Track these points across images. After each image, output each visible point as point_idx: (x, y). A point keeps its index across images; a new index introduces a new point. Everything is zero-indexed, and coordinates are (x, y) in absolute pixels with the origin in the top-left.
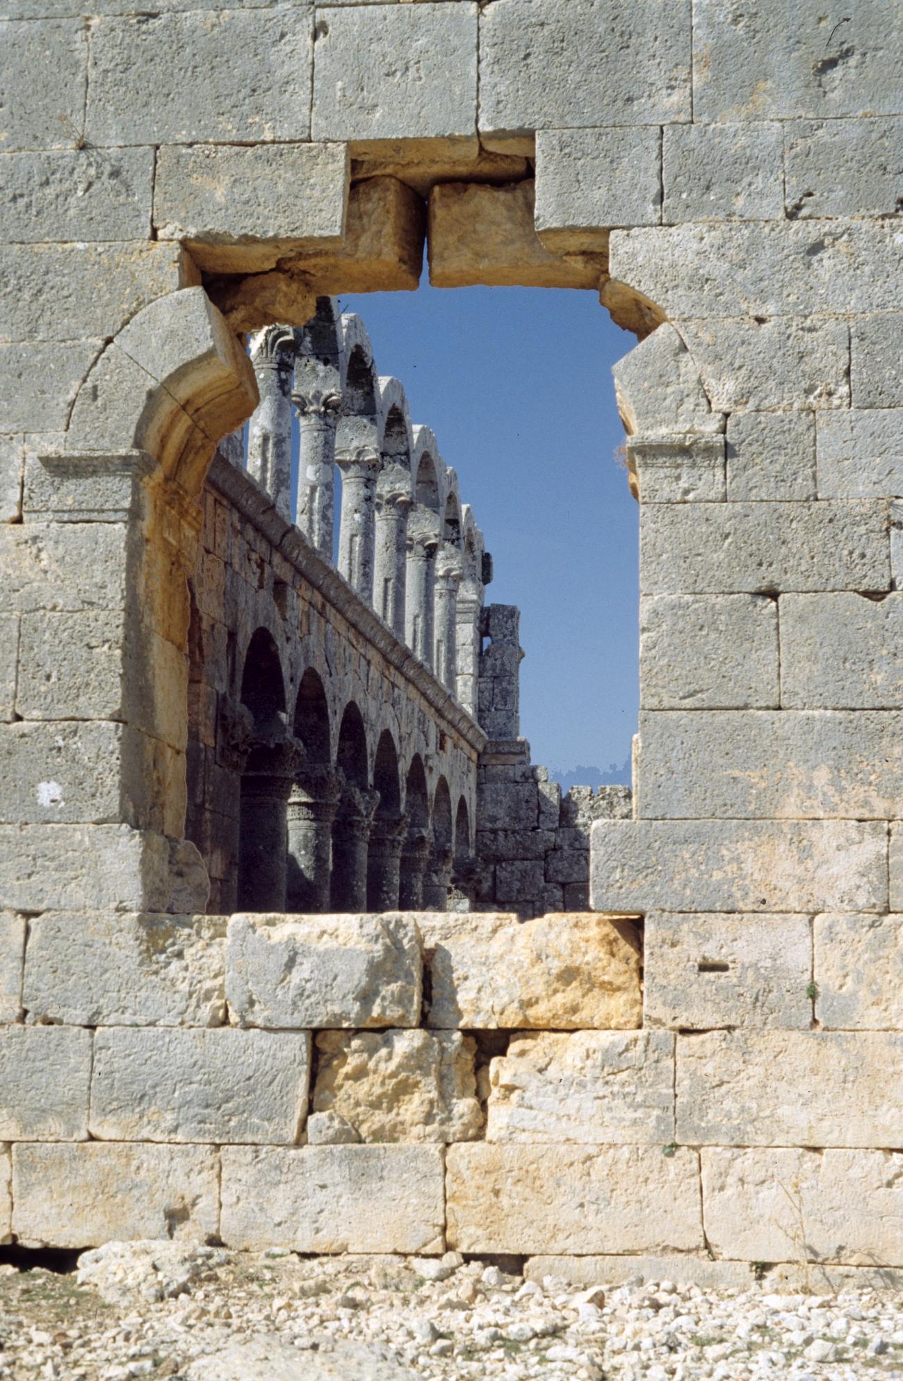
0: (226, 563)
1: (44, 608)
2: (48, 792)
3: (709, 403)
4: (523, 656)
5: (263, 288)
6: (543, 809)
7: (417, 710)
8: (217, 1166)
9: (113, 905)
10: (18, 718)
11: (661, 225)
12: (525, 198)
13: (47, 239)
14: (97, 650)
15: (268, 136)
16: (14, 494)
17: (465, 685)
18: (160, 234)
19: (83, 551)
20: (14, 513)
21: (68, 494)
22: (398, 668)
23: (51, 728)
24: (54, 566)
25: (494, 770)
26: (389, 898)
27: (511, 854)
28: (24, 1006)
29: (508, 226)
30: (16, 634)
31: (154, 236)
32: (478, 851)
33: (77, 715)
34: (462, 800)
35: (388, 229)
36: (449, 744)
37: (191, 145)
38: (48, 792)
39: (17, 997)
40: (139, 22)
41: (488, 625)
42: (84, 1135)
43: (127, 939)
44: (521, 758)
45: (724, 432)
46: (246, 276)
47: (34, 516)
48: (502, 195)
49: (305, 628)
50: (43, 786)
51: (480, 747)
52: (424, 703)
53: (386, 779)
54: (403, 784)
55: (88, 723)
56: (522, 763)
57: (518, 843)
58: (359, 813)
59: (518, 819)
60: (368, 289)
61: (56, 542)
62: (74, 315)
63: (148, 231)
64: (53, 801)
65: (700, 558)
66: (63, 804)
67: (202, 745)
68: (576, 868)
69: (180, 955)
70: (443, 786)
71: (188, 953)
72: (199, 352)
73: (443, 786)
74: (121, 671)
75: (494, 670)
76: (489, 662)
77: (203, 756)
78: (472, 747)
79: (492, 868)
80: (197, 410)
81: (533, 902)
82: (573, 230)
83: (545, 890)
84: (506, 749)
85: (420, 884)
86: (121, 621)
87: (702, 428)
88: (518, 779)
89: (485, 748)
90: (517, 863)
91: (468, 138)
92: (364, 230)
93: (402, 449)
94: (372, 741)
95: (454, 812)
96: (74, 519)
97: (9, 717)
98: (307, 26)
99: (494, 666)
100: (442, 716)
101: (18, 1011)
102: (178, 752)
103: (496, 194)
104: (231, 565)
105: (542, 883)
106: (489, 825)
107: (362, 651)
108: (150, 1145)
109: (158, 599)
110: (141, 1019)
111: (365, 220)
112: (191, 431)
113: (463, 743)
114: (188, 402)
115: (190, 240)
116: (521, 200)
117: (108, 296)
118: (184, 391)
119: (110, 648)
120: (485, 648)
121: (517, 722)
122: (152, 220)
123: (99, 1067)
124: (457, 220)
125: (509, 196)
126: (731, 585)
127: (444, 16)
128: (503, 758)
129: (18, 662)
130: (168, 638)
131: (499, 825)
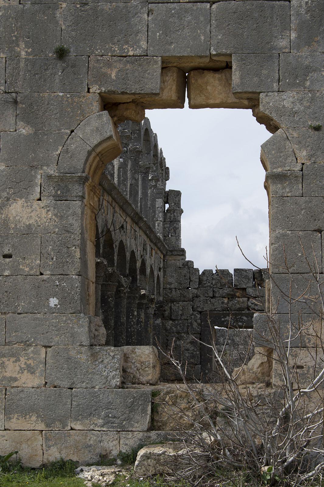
1: (50, 232)
2: (53, 302)
3: (297, 159)
5: (127, 109)
6: (192, 279)
7: (143, 240)
8: (119, 439)
9: (78, 344)
10: (41, 274)
11: (279, 91)
12: (225, 76)
13: (47, 91)
14: (71, 249)
15: (131, 53)
16: (38, 189)
18: (91, 90)
19: (64, 212)
20: (38, 196)
21: (58, 190)
23: (54, 278)
24: (54, 217)
28: (46, 381)
29: (220, 88)
30: (40, 242)
31: (88, 92)
32: (164, 297)
33: (64, 273)
34: (158, 275)
35: (174, 87)
36: (154, 252)
37: (102, 56)
38: (53, 302)
39: (43, 378)
40: (80, 6)
41: (168, 199)
42: (69, 428)
43: (84, 357)
44: (182, 257)
45: (302, 170)
46: (120, 103)
47: (45, 198)
48: (217, 76)
49: (106, 212)
50: (51, 299)
51: (165, 254)
53: (133, 271)
54: (138, 272)
55: (67, 276)
56: (182, 259)
58: (123, 286)
59: (180, 284)
60: (165, 108)
61: (54, 208)
62: (59, 121)
63: (86, 90)
64: (55, 305)
65: (293, 217)
66: (59, 306)
68: (206, 305)
69: (102, 361)
70: (152, 271)
71: (106, 361)
72: (106, 137)
73: (152, 271)
74: (80, 257)
76: (169, 215)
78: (162, 253)
79: (170, 304)
80: (102, 155)
81: (187, 320)
82: (246, 92)
83: (193, 314)
84: (176, 253)
85: (143, 314)
86: (80, 238)
87: (294, 169)
88: (181, 266)
89: (167, 253)
91: (206, 56)
92: (165, 88)
93: (137, 128)
95: (156, 282)
96: (61, 199)
97: (38, 273)
98: (145, 9)
99: (170, 217)
100: (151, 241)
101: (44, 383)
102: (93, 283)
103: (215, 75)
105: (191, 312)
108: (94, 431)
109: (88, 226)
110: (89, 386)
111: (166, 84)
112: (98, 162)
113: (159, 252)
114: (100, 152)
115: (102, 93)
116: (224, 77)
117: (72, 114)
118: (99, 150)
119: (75, 248)
120: (166, 209)
121: (180, 241)
122: (88, 85)
123: (74, 403)
124: (200, 85)
125: (220, 76)
126: (304, 228)
127: (197, 8)
128: (174, 257)
129: (41, 253)
130: (91, 241)
131: (173, 286)
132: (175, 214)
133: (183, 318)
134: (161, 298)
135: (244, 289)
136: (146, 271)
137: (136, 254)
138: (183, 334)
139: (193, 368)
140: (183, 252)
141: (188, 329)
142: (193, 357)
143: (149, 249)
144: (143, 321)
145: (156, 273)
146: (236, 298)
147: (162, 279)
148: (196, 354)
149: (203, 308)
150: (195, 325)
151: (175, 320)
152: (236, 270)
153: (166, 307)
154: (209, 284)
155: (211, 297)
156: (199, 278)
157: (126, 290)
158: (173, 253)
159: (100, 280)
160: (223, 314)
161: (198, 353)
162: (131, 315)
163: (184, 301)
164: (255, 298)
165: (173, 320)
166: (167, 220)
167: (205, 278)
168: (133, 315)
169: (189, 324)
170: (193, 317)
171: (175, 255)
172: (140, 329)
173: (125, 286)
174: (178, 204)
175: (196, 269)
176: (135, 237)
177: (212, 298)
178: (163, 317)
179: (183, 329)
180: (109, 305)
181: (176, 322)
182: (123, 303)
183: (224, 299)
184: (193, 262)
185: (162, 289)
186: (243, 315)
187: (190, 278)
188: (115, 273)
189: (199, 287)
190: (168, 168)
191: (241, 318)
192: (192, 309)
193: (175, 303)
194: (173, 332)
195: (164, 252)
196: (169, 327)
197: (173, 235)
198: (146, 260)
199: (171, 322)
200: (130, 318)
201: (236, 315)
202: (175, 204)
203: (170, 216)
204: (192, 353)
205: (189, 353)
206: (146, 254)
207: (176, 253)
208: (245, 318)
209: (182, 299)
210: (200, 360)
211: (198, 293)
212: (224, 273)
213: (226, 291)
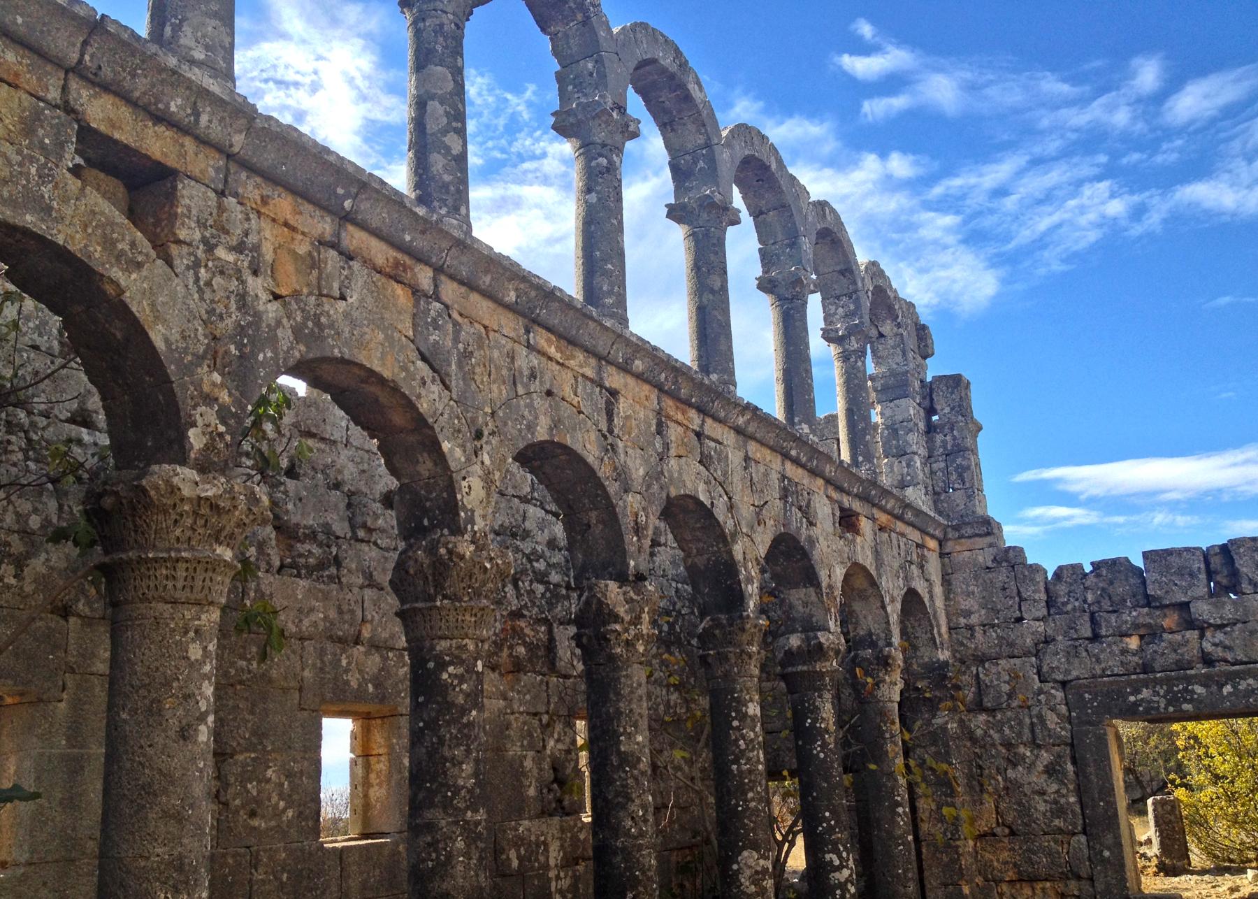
4: (980, 429)
6: (1024, 595)
7: (774, 476)
17: (908, 466)
22: (701, 410)
25: (961, 557)
26: (743, 737)
32: (954, 652)
36: (865, 525)
41: (932, 400)
44: (989, 539)
56: (991, 545)
58: (616, 618)
68: (1077, 660)
75: (945, 447)
78: (924, 532)
79: (974, 669)
81: (1029, 708)
83: (1040, 692)
84: (969, 531)
85: (828, 706)
88: (990, 564)
89: (945, 534)
99: (944, 443)
100: (840, 489)
105: (1037, 684)
106: (962, 621)
107: (589, 372)
113: (900, 526)
131: (974, 619)
133: (1015, 704)
135: (1184, 607)
137: (720, 513)
138: (1022, 749)
139: (1066, 846)
140: (989, 528)
141: (1033, 731)
142: (1059, 811)
143: (824, 510)
144: (832, 728)
145: (892, 587)
146: (1165, 635)
147: (938, 603)
148: (1068, 803)
149: (1067, 672)
152: (1146, 555)
155: (1087, 639)
156: (1047, 590)
157: (632, 632)
159: (180, 584)
160: (1130, 683)
161: (1072, 799)
162: (735, 718)
164: (1220, 627)
165: (991, 711)
166: (936, 453)
167: (1062, 589)
168: (743, 717)
169: (1035, 720)
170: (1042, 697)
171: (969, 537)
172: (822, 755)
173: (627, 618)
174: (963, 408)
175: (1031, 566)
179: (1020, 735)
180: (445, 697)
181: (999, 717)
182: (623, 680)
184: (1021, 550)
185: (944, 629)
186: (1189, 680)
187: (1019, 593)
189: (1049, 615)
191: (1186, 689)
192: (1036, 677)
195: (938, 533)
196: (979, 732)
197: (956, 486)
198: (812, 541)
199: (982, 717)
200: (733, 728)
201: (1168, 681)
202: (952, 409)
203: (943, 441)
204: (1056, 802)
205: (1045, 801)
206: (811, 524)
207: (968, 531)
208: (1199, 689)
210: (1081, 822)
211: (1050, 632)
212: (1112, 568)
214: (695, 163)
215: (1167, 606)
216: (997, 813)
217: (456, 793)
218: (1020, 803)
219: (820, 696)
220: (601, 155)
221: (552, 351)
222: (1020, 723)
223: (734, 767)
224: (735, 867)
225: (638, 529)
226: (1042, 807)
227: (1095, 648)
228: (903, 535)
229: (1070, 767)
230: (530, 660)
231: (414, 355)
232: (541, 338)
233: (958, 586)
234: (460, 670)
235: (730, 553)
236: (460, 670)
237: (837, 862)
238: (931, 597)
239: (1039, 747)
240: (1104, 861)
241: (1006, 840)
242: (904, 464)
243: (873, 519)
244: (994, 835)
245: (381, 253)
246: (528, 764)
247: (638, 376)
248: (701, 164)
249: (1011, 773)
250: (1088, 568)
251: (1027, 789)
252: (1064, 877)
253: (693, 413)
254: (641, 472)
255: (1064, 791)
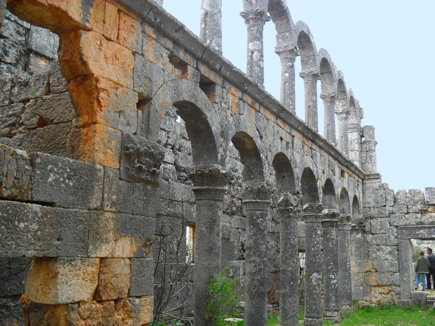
0: (134, 53)
4: (377, 143)
7: (327, 160)
17: (355, 155)
26: (316, 240)
27: (376, 216)
36: (346, 175)
41: (363, 133)
52: (331, 159)
54: (320, 191)
56: (378, 182)
57: (378, 211)
58: (292, 205)
59: (378, 203)
67: (98, 166)
77: (101, 174)
78: (359, 177)
79: (369, 221)
81: (385, 233)
84: (372, 177)
85: (334, 231)
88: (378, 188)
90: (379, 219)
93: (312, 54)
94: (298, 172)
95: (351, 201)
100: (341, 164)
104: (143, 55)
105: (389, 227)
107: (289, 131)
113: (354, 175)
128: (371, 181)
131: (371, 205)
132: (370, 145)
134: (361, 216)
136: (334, 191)
137: (315, 172)
138: (382, 246)
141: (386, 241)
142: (392, 266)
143: (338, 171)
145: (351, 195)
146: (429, 214)
147: (361, 200)
149: (399, 223)
150: (392, 238)
151: (374, 234)
152: (427, 189)
153: (367, 223)
154: (403, 202)
156: (394, 198)
157: (296, 209)
158: (370, 177)
160: (417, 228)
161: (396, 262)
163: (382, 218)
167: (399, 197)
169: (387, 238)
170: (390, 231)
172: (332, 246)
176: (312, 155)
177: (406, 214)
178: (364, 232)
180: (259, 227)
182: (292, 223)
183: (417, 214)
185: (362, 208)
187: (386, 198)
188: (265, 188)
190: (361, 109)
193: (374, 219)
194: (374, 245)
196: (369, 240)
197: (369, 162)
198: (334, 181)
199: (371, 236)
200: (313, 237)
201: (429, 228)
202: (369, 136)
204: (391, 263)
206: (334, 175)
209: (380, 216)
211: (394, 210)
213: (419, 206)
214: (309, 61)
215: (430, 205)
216: (373, 265)
217: (261, 253)
218: (380, 263)
219: (332, 229)
220: (290, 62)
221: (281, 125)
222: (382, 238)
223: (313, 249)
224: (311, 277)
225: (298, 178)
226: (386, 264)
227: (407, 216)
228: (354, 178)
229: (396, 252)
230: (237, 212)
231: (256, 129)
232: (279, 122)
233: (367, 194)
234: (262, 220)
235: (316, 185)
236: (262, 220)
237: (333, 278)
238: (359, 199)
239: (387, 245)
240: (404, 281)
241: (375, 273)
242: (354, 154)
243: (348, 173)
244: (371, 272)
245: (250, 100)
246: (236, 244)
247: (299, 132)
248: (311, 61)
249: (378, 253)
250: (407, 191)
251: (382, 258)
252: (391, 285)
253: (310, 142)
254: (299, 161)
255: (394, 259)
